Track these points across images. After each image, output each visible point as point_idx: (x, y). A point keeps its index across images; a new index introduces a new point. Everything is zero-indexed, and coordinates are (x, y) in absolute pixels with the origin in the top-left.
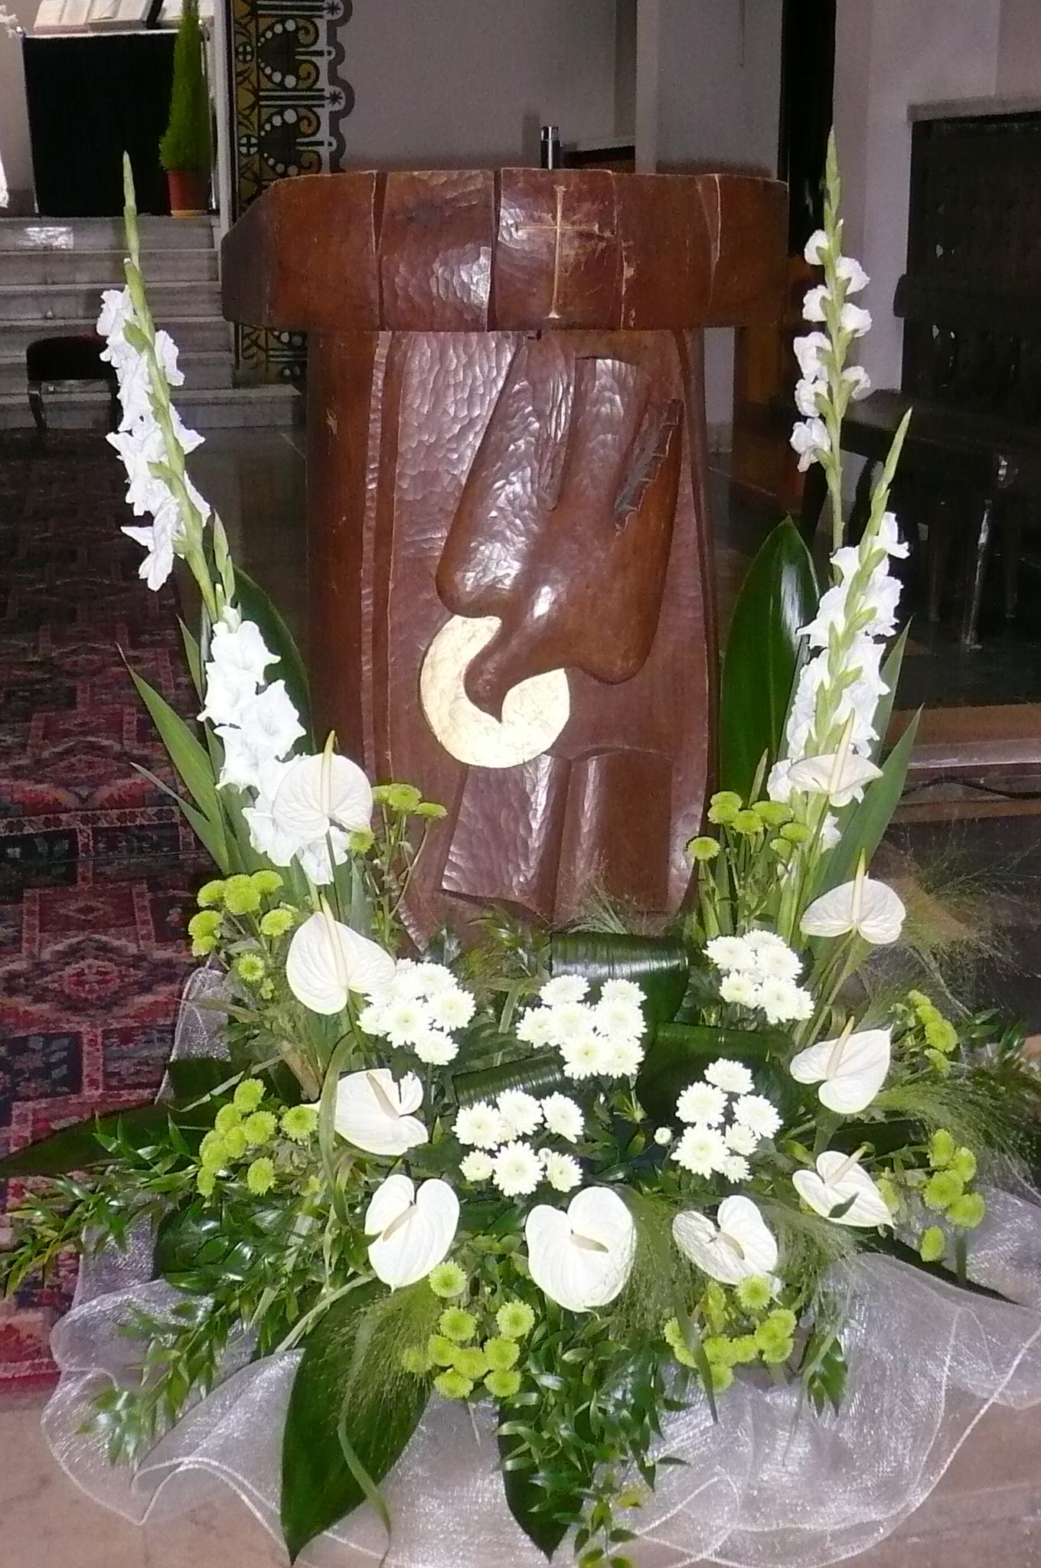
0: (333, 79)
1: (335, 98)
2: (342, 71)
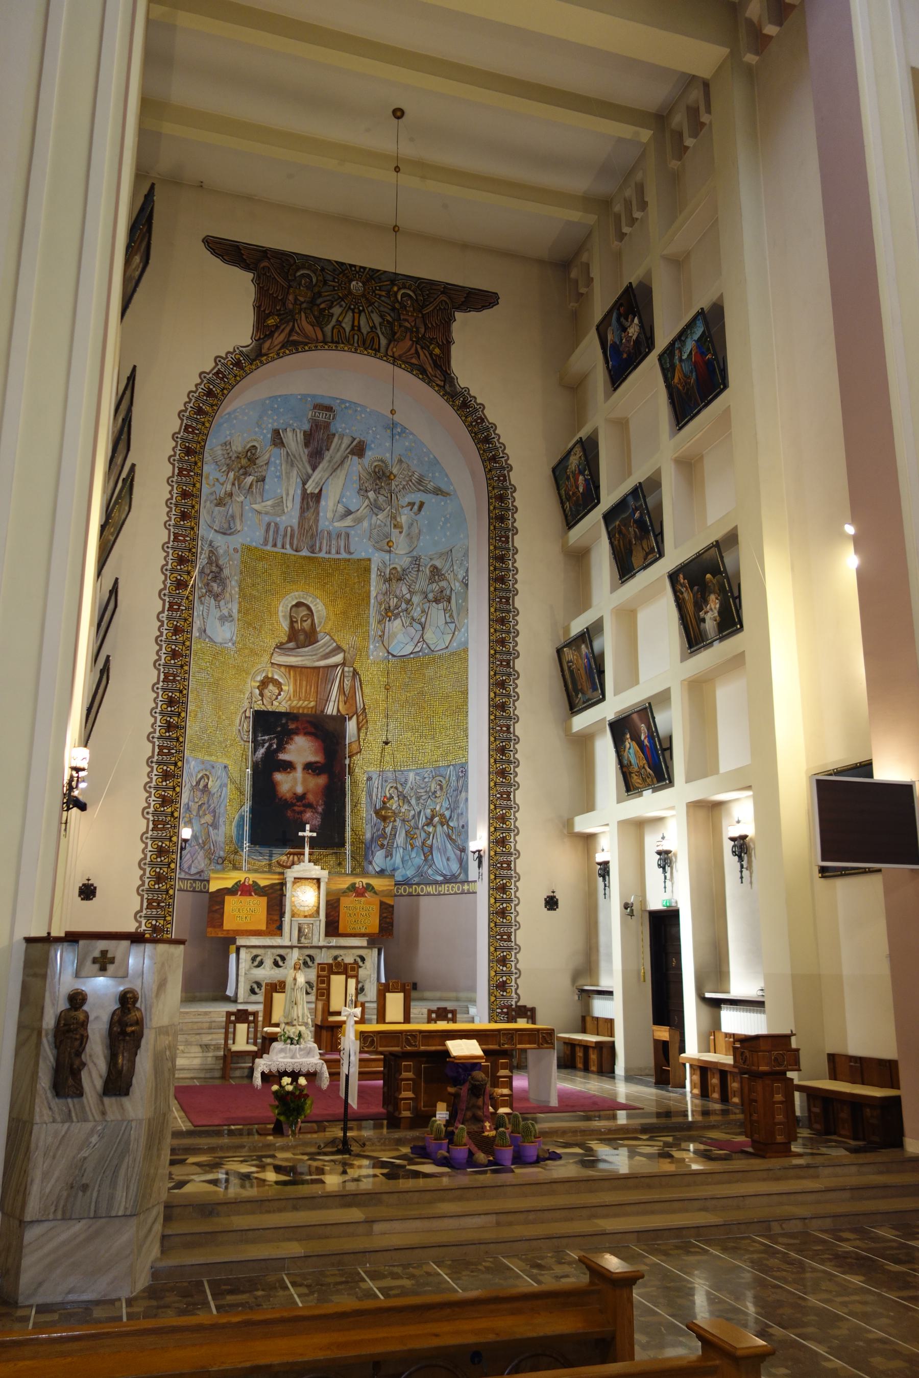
0: (516, 968)
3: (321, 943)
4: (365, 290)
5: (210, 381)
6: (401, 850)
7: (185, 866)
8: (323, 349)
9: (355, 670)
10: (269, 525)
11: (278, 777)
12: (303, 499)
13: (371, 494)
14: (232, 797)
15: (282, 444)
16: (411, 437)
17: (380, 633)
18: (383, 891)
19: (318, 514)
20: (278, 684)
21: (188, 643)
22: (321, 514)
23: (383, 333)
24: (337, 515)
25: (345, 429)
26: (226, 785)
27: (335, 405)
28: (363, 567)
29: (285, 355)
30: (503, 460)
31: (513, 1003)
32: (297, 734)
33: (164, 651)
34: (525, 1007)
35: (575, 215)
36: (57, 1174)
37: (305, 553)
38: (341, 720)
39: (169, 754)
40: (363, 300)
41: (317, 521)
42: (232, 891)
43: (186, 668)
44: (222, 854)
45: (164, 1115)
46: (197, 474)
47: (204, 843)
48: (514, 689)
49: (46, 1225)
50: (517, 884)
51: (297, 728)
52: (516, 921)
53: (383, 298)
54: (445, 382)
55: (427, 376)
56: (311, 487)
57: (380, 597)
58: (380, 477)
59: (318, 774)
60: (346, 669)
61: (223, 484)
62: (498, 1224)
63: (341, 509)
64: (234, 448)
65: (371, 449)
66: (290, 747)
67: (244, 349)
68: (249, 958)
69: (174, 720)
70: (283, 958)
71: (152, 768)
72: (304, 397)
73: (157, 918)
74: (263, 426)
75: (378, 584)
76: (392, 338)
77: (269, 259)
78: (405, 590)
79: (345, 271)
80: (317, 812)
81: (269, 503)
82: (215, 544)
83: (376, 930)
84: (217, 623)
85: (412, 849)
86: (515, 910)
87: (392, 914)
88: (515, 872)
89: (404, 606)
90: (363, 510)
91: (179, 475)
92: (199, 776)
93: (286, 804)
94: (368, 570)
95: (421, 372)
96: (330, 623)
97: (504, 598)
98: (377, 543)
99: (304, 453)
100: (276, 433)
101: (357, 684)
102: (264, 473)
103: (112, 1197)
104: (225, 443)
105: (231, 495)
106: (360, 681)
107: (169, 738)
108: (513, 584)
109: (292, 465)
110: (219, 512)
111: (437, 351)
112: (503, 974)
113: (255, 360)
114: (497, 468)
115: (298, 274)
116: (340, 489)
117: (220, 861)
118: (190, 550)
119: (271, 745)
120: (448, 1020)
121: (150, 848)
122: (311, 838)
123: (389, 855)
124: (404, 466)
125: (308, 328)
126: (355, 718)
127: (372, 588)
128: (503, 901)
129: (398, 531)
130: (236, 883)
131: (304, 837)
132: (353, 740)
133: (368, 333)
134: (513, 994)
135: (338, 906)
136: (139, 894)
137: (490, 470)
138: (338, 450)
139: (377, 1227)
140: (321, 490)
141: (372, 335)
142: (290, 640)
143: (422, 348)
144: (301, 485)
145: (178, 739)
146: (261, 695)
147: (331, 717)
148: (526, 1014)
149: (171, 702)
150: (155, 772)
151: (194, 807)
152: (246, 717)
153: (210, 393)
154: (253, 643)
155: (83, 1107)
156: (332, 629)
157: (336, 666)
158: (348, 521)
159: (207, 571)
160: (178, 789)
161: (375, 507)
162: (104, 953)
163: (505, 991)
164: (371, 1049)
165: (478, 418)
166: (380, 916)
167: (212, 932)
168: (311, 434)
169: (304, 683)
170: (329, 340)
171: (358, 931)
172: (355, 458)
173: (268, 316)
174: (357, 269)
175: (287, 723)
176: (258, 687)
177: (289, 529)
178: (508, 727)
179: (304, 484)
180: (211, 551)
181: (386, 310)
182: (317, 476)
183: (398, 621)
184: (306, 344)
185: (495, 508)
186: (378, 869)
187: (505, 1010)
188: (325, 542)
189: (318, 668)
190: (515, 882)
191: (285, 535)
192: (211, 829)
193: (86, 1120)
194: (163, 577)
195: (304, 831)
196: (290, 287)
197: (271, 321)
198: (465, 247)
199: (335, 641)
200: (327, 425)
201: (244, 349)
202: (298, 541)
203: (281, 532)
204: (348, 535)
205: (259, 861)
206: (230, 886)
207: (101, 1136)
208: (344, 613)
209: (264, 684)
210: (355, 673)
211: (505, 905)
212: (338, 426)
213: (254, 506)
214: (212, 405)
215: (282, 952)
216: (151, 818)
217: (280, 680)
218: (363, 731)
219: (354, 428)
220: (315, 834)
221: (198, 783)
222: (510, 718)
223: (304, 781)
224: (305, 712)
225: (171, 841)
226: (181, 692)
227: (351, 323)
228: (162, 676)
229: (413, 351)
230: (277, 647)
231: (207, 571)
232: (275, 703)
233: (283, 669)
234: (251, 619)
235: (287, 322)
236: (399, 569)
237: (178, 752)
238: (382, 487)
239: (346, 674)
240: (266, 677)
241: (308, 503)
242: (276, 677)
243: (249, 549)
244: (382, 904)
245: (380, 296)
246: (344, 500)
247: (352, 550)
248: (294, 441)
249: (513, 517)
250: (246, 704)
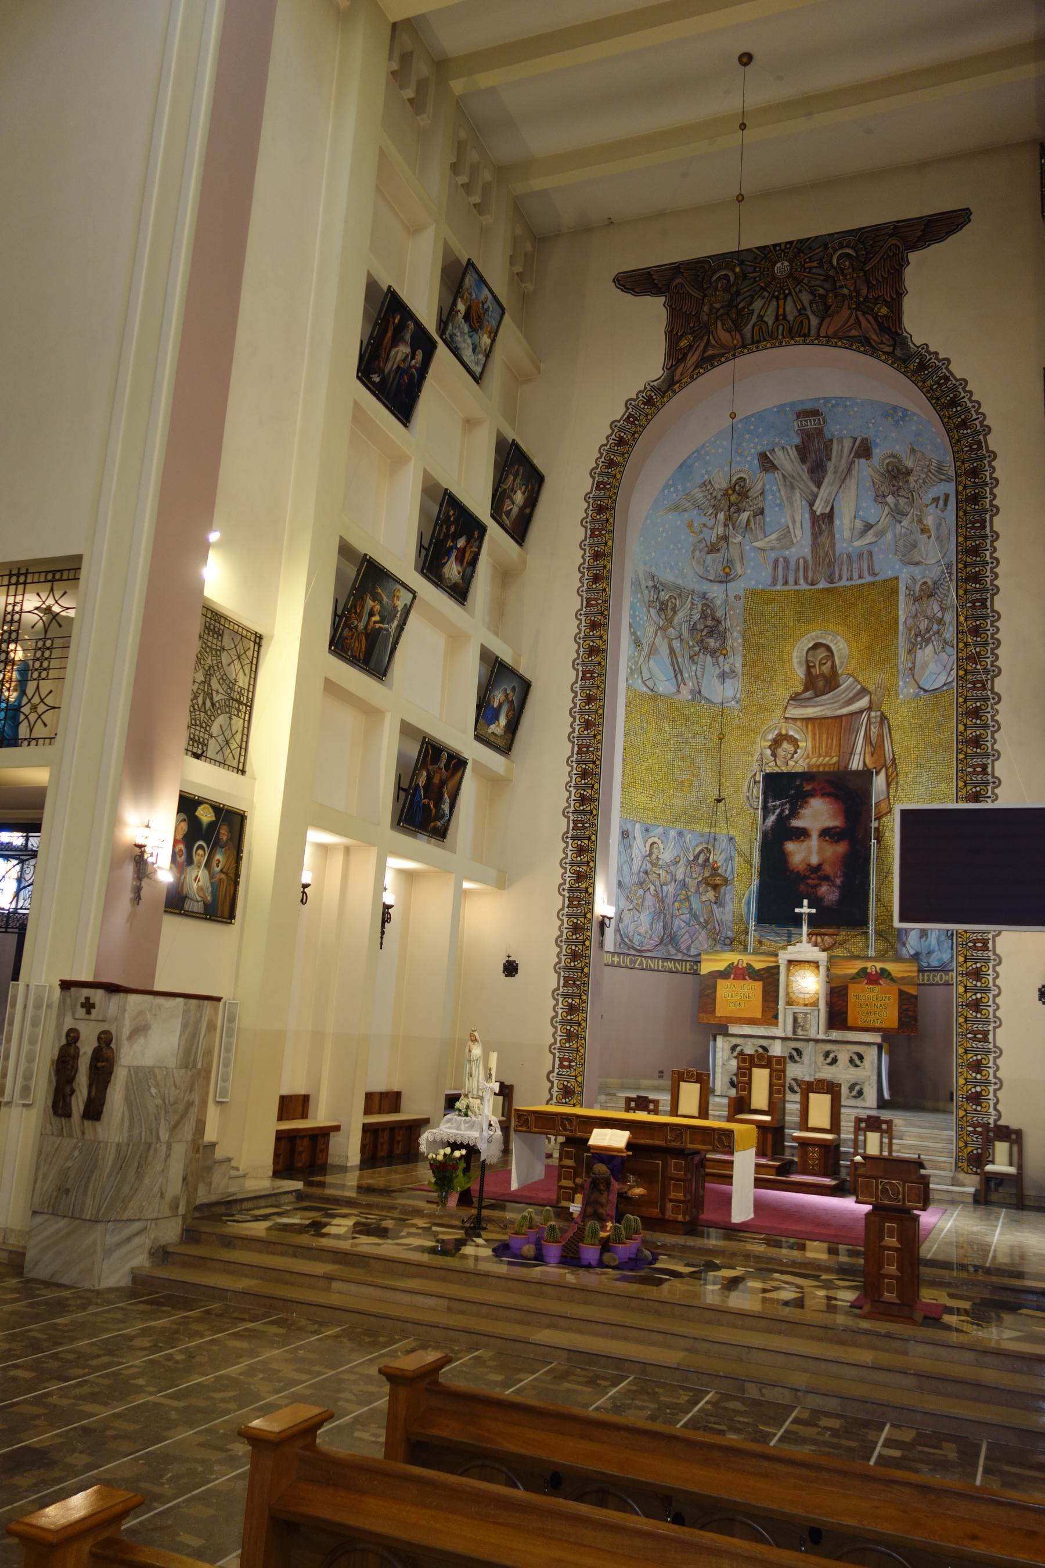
0: (995, 1077)
1: (995, 1084)
2: (998, 1074)
3: (821, 1036)
4: (791, 268)
5: (621, 429)
7: (683, 947)
8: (742, 354)
9: (882, 714)
10: (776, 561)
11: (790, 846)
12: (813, 523)
13: (890, 499)
14: (740, 871)
15: (775, 467)
16: (915, 418)
17: (910, 665)
18: (903, 978)
19: (833, 536)
20: (794, 741)
21: (600, 711)
22: (837, 536)
23: (813, 313)
24: (856, 533)
25: (842, 430)
26: (731, 858)
27: (820, 406)
28: (890, 589)
29: (699, 375)
30: (977, 422)
31: (991, 1121)
32: (813, 796)
33: (577, 722)
34: (1007, 1127)
35: (1027, 72)
36: (51, 1178)
37: (822, 585)
38: (866, 775)
39: (584, 828)
40: (790, 282)
41: (833, 545)
42: (724, 975)
43: (599, 737)
44: (730, 934)
45: (149, 1145)
46: (608, 532)
47: (706, 922)
48: (993, 717)
49: (44, 1217)
50: (998, 968)
51: (814, 790)
52: (995, 1016)
53: (814, 270)
54: (894, 346)
55: (871, 346)
56: (820, 508)
57: (910, 621)
58: (896, 475)
59: (837, 842)
60: (873, 714)
61: (712, 528)
62: (450, 1310)
63: (859, 524)
64: (717, 486)
65: (877, 445)
66: (805, 812)
67: (655, 383)
68: (728, 1047)
69: (588, 793)
70: (861, 1057)
71: (567, 843)
72: (781, 408)
73: (573, 996)
74: (746, 453)
75: (906, 605)
76: (825, 313)
77: (682, 273)
78: (936, 608)
79: (767, 254)
80: (835, 886)
81: (773, 536)
82: (710, 595)
83: (895, 1025)
84: (716, 682)
86: (994, 1002)
87: (916, 1006)
88: (995, 954)
89: (935, 627)
90: (885, 520)
91: (591, 536)
92: (698, 850)
93: (799, 877)
94: (895, 591)
95: (864, 344)
96: (854, 662)
97: (978, 600)
98: (904, 555)
99: (802, 470)
100: (763, 457)
101: (886, 730)
102: (760, 505)
103: (83, 1203)
104: (704, 483)
105: (725, 538)
106: (889, 726)
107: (583, 812)
108: (992, 581)
109: (792, 487)
110: (714, 560)
111: (884, 311)
112: (976, 1083)
113: (667, 391)
114: (968, 435)
115: (714, 278)
116: (853, 502)
117: (728, 941)
118: (602, 613)
119: (782, 811)
120: (649, 1112)
121: (566, 925)
122: (809, 914)
124: (919, 455)
125: (724, 336)
126: (883, 771)
127: (901, 612)
128: (976, 990)
129: (925, 536)
130: (729, 966)
131: (801, 914)
132: (882, 798)
133: (796, 317)
134: (991, 1110)
135: (846, 994)
136: (556, 972)
137: (959, 441)
138: (841, 456)
139: (335, 1285)
140: (832, 508)
141: (801, 318)
142: (806, 690)
143: (864, 313)
144: (808, 509)
145: (591, 812)
146: (774, 755)
147: (857, 773)
148: (647, 1106)
149: (584, 774)
150: (570, 848)
151: (692, 884)
152: (756, 782)
153: (621, 442)
154: (763, 698)
155: (71, 1126)
156: (855, 669)
157: (861, 712)
158: (870, 537)
159: (700, 626)
160: (592, 864)
161: (898, 514)
162: (87, 999)
163: (979, 1104)
164: (524, 1129)
165: (941, 378)
166: (900, 1008)
167: (705, 1018)
168: (804, 447)
169: (825, 736)
170: (749, 341)
171: (871, 1025)
172: (863, 461)
173: (680, 339)
174: (783, 247)
175: (801, 784)
176: (770, 747)
177: (801, 561)
178: (984, 767)
179: (811, 505)
180: (704, 605)
181: (818, 283)
182: (824, 492)
183: (930, 647)
184: (722, 355)
185: (965, 488)
186: (912, 952)
187: (979, 1129)
188: (845, 567)
189: (841, 717)
190: (994, 966)
191: (797, 569)
192: (715, 906)
193: (71, 1136)
194: (576, 646)
195: (802, 907)
196: (705, 296)
197: (684, 343)
198: (922, 165)
199: (859, 683)
200: (820, 432)
201: (655, 383)
202: (814, 572)
203: (792, 563)
204: (870, 554)
205: (776, 942)
206: (722, 969)
207: (81, 1152)
208: (870, 647)
209: (776, 743)
210: (883, 717)
211: (979, 996)
212: (833, 429)
213: (756, 544)
214: (623, 454)
215: (764, 1042)
216: (567, 895)
217: (797, 736)
218: (893, 786)
219: (851, 427)
220: (814, 911)
221: (697, 857)
222: (987, 755)
223: (820, 850)
224: (827, 769)
225: (585, 918)
226: (594, 763)
227: (774, 314)
228: (576, 749)
229: (852, 321)
230: (792, 699)
231: (700, 626)
232: (791, 763)
233: (799, 723)
234: (758, 672)
235: (701, 338)
236: (930, 583)
237: (592, 825)
238: (900, 488)
239: (873, 720)
240: (780, 734)
241: (819, 527)
242: (791, 733)
243: (754, 593)
244: (901, 993)
245: (811, 268)
246: (861, 513)
247: (877, 571)
248: (787, 460)
249: (991, 493)
250: (755, 767)
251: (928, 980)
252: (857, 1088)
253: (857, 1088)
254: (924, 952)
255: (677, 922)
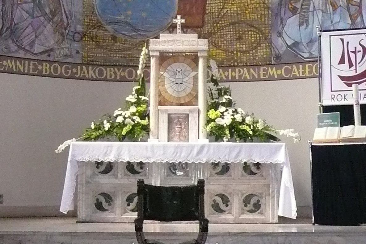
6: (320, 14)
7: (26, 42)
44: (79, 28)
47: (53, 14)
85: (335, 9)
117: (77, 37)
123: (304, 22)
186: (290, 42)
251: (310, 72)
252: (253, 201)
253: (253, 201)
254: (304, 42)
255: (18, 13)
